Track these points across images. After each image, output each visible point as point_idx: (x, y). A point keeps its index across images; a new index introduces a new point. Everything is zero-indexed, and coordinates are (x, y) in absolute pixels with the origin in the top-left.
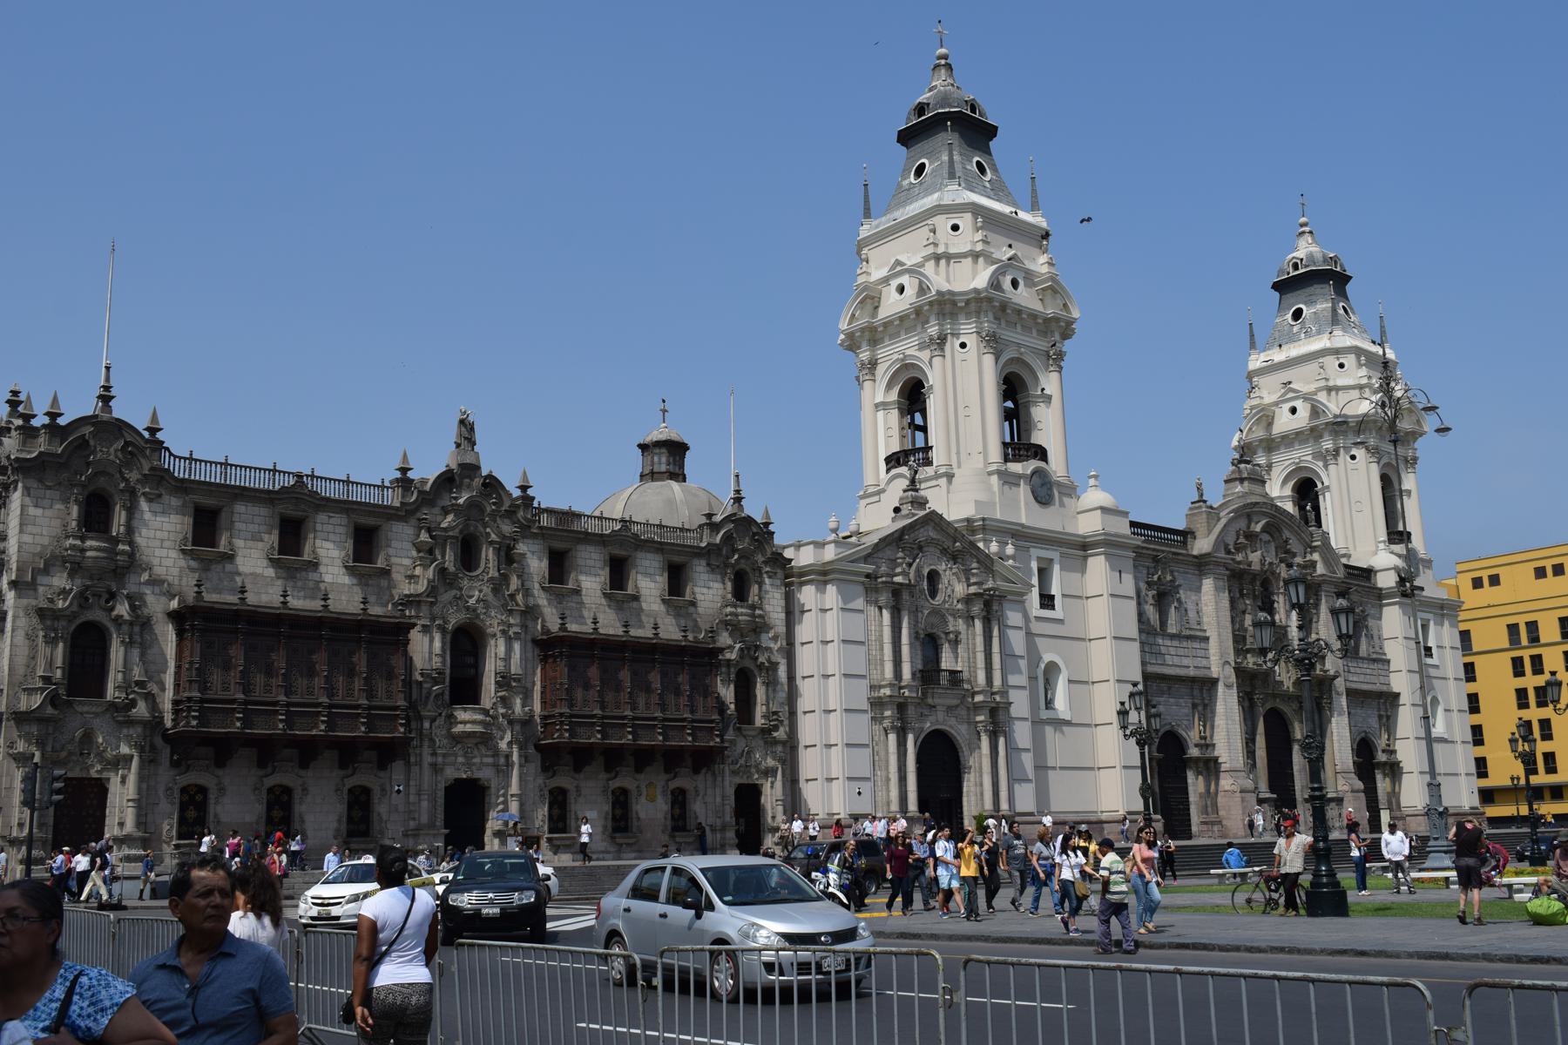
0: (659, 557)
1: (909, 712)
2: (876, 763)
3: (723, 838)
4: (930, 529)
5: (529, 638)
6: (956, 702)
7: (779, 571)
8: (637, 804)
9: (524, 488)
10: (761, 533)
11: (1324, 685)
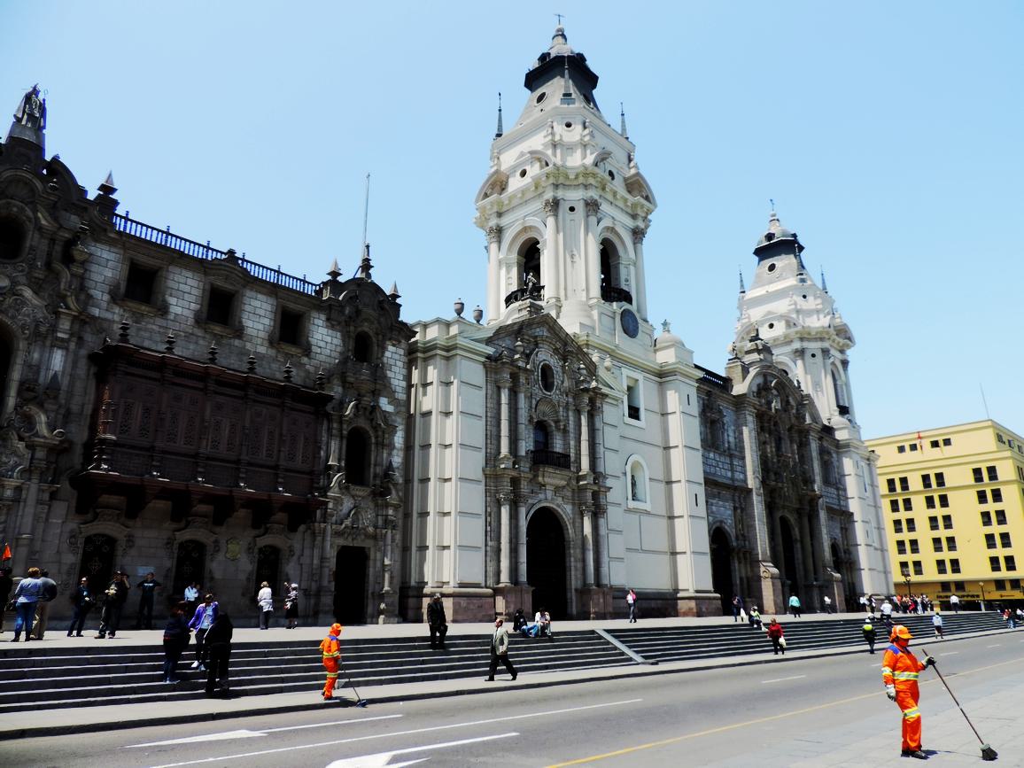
0: (272, 301)
1: (522, 486)
2: (489, 533)
3: (317, 604)
5: (83, 352)
6: (564, 483)
7: (403, 341)
8: (212, 561)
9: (107, 189)
10: (389, 304)
11: (813, 501)
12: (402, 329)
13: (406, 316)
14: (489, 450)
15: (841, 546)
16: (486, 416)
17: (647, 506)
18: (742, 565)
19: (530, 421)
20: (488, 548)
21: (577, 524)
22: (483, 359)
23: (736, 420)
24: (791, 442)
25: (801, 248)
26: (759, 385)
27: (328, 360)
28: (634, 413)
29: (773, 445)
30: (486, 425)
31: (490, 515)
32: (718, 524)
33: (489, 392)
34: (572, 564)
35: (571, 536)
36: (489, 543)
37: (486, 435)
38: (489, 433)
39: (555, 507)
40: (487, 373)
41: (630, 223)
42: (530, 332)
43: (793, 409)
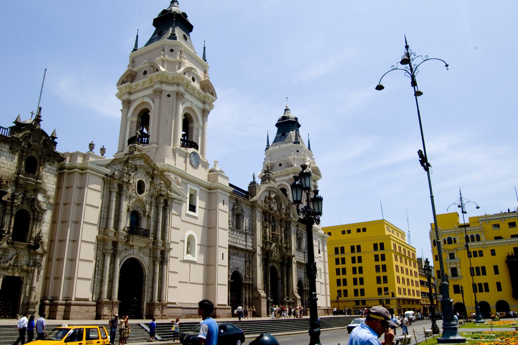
1: (119, 246)
2: (97, 271)
4: (142, 161)
6: (144, 245)
7: (56, 163)
11: (290, 259)
12: (56, 156)
13: (60, 149)
14: (101, 226)
15: (304, 282)
16: (102, 207)
17: (195, 259)
18: (247, 291)
19: (128, 210)
20: (96, 280)
21: (151, 268)
22: (103, 176)
23: (251, 215)
24: (281, 227)
25: (299, 126)
26: (266, 197)
27: (8, 171)
28: (192, 208)
29: (271, 228)
30: (101, 212)
31: (99, 261)
32: (235, 269)
33: (105, 193)
34: (146, 289)
35: (147, 274)
36: (96, 277)
37: (101, 217)
38: (102, 216)
39: (138, 258)
40: (104, 183)
41: (201, 105)
42: (133, 162)
43: (283, 210)
